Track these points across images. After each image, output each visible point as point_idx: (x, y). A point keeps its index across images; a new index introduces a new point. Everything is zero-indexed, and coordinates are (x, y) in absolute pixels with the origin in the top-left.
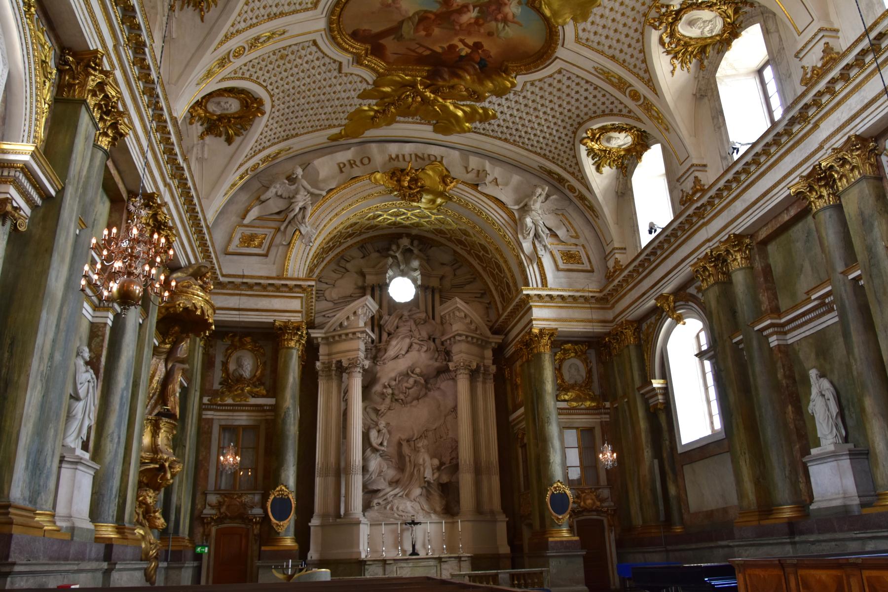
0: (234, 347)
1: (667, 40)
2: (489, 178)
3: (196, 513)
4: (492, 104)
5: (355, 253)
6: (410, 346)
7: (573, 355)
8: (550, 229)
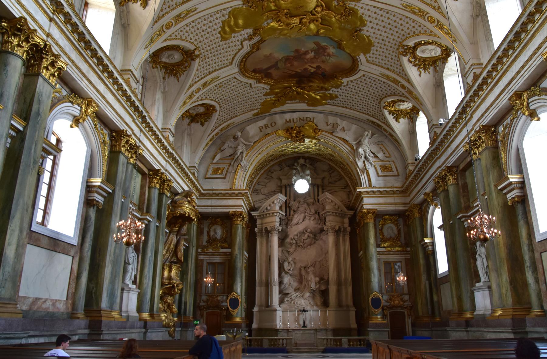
0: (213, 224)
1: (413, 60)
2: (340, 127)
4: (333, 91)
5: (277, 168)
6: (305, 217)
7: (389, 222)
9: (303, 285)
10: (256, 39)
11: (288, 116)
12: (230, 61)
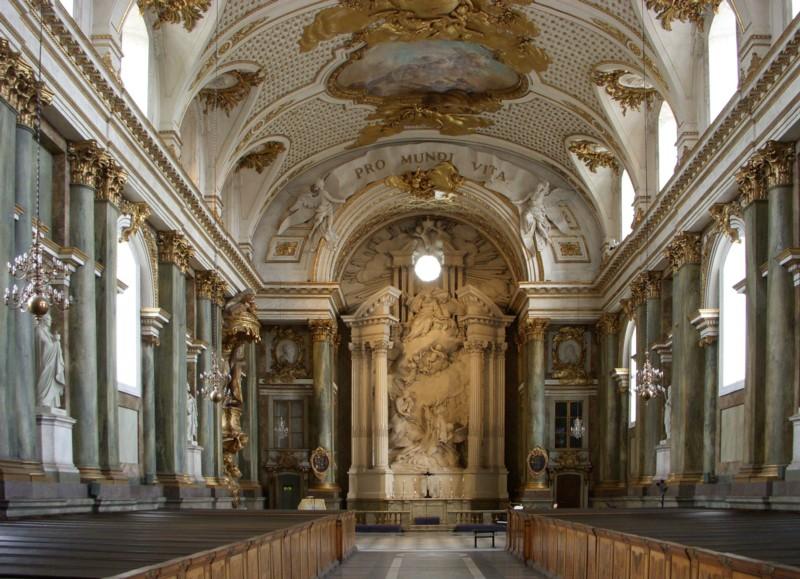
0: (278, 338)
1: (614, 90)
2: (497, 173)
3: (262, 464)
4: (486, 115)
5: (385, 234)
8: (550, 222)
9: (427, 436)
10: (358, 46)
11: (406, 150)
12: (312, 77)
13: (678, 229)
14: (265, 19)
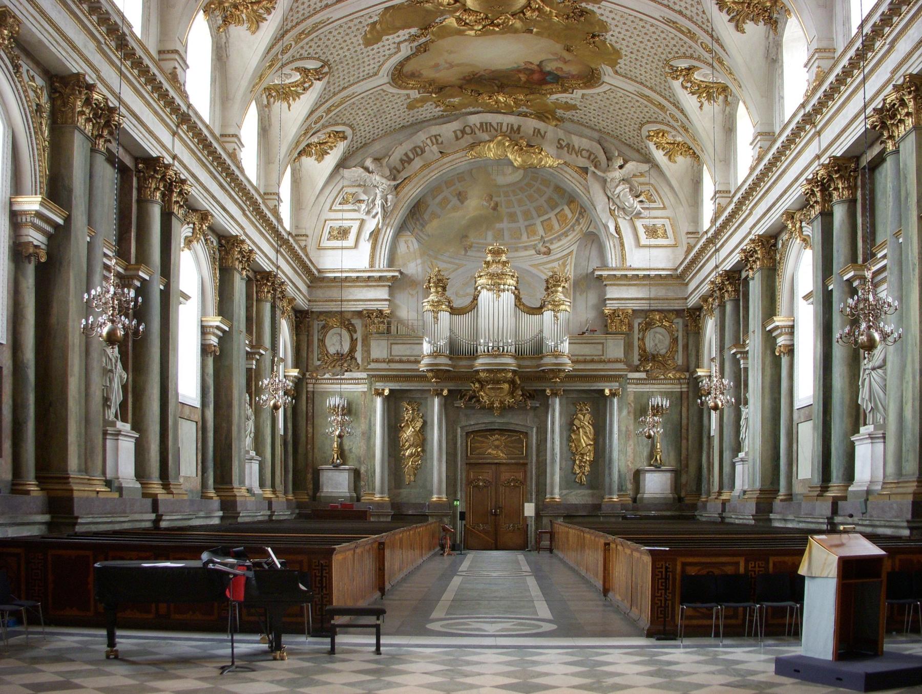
13: (753, 232)
14: (328, 19)
